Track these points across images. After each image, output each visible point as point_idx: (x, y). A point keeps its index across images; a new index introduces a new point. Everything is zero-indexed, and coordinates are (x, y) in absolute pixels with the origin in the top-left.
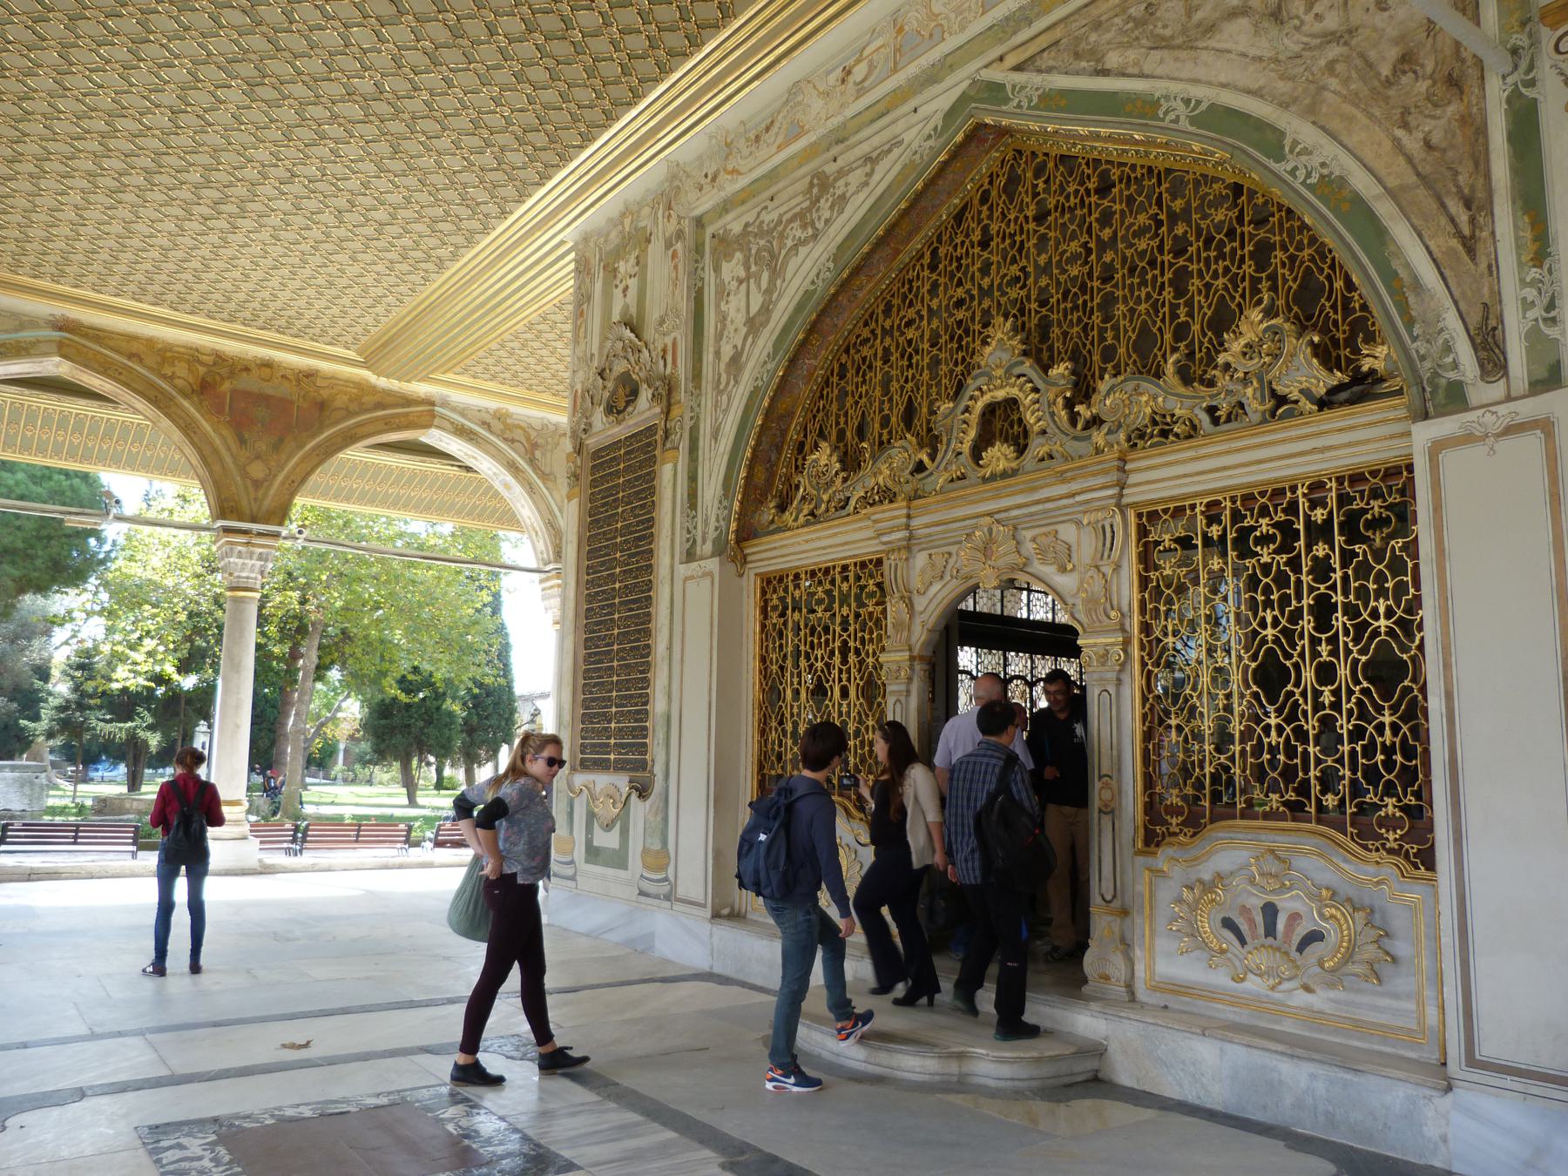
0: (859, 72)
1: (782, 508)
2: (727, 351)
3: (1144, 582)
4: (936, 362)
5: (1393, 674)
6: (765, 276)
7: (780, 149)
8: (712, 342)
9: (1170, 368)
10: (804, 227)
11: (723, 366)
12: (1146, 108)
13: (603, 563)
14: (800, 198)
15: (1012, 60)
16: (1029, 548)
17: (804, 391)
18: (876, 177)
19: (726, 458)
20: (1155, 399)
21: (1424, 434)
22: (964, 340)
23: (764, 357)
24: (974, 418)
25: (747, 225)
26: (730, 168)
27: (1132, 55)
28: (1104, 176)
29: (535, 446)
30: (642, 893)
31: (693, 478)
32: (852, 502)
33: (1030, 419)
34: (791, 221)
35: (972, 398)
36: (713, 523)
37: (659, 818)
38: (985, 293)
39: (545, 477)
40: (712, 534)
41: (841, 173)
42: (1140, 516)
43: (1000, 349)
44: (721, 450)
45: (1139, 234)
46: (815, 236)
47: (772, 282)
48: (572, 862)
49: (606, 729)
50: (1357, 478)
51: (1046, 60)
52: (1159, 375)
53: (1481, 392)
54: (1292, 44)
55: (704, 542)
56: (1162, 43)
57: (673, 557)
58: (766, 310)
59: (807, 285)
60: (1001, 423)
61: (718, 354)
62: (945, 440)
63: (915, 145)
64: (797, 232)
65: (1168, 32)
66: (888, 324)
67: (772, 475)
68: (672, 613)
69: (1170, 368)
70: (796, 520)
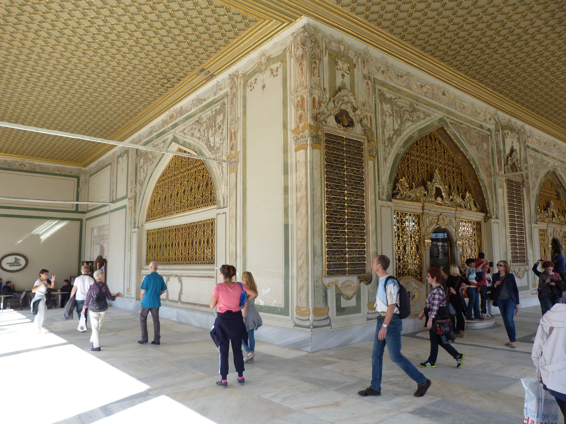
2: (387, 135)
6: (399, 120)
7: (405, 87)
11: (386, 139)
12: (467, 151)
13: (337, 186)
14: (408, 106)
18: (426, 120)
24: (434, 188)
26: (389, 75)
30: (368, 319)
33: (443, 194)
36: (386, 190)
44: (388, 166)
48: (328, 318)
49: (343, 258)
52: (459, 195)
53: (493, 217)
55: (383, 194)
56: (467, 140)
57: (375, 196)
60: (438, 193)
61: (383, 132)
62: (430, 191)
63: (434, 120)
68: (376, 216)
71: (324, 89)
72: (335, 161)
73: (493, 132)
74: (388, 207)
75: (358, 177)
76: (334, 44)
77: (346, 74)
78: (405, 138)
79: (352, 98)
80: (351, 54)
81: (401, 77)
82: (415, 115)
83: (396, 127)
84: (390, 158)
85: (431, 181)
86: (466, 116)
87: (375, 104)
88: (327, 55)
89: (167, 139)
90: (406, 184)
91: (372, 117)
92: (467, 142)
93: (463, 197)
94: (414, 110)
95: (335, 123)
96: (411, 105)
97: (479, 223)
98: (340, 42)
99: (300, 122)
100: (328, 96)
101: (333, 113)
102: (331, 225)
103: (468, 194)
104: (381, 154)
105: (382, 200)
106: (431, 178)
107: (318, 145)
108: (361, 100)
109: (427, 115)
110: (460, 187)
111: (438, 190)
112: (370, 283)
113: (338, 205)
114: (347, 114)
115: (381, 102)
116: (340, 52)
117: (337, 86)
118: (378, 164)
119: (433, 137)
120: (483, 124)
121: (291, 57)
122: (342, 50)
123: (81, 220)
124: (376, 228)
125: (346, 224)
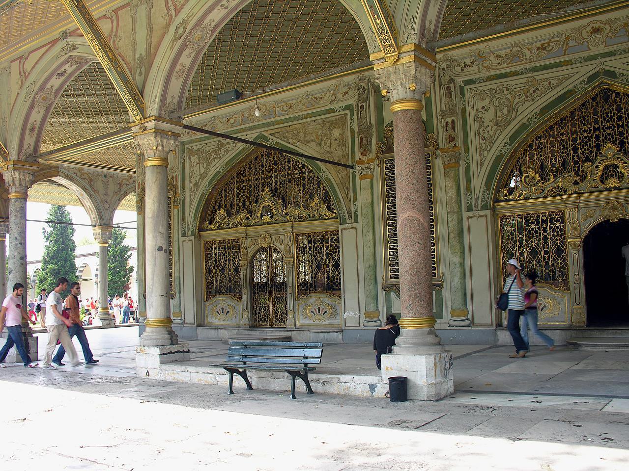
0: (232, 121)
1: (210, 224)
2: (193, 182)
3: (297, 248)
4: (250, 192)
5: (337, 266)
6: (205, 165)
8: (188, 177)
9: (301, 206)
10: (217, 154)
15: (269, 132)
16: (274, 239)
17: (215, 194)
18: (236, 148)
20: (299, 211)
21: (341, 227)
22: (258, 189)
25: (199, 148)
27: (294, 141)
28: (289, 159)
29: (91, 180)
31: (184, 213)
32: (230, 225)
34: (212, 152)
35: (260, 204)
38: (263, 178)
39: (95, 191)
40: (191, 230)
42: (296, 235)
45: (297, 174)
47: (207, 166)
50: (332, 231)
51: (277, 135)
53: (348, 221)
54: (322, 151)
55: (188, 232)
57: (179, 235)
58: (206, 173)
59: (218, 169)
61: (190, 181)
64: (214, 155)
65: (301, 139)
66: (238, 180)
67: (206, 214)
69: (301, 206)
70: (215, 227)
86: (295, 115)
91: (178, 175)
115: (189, 158)
120: (329, 107)
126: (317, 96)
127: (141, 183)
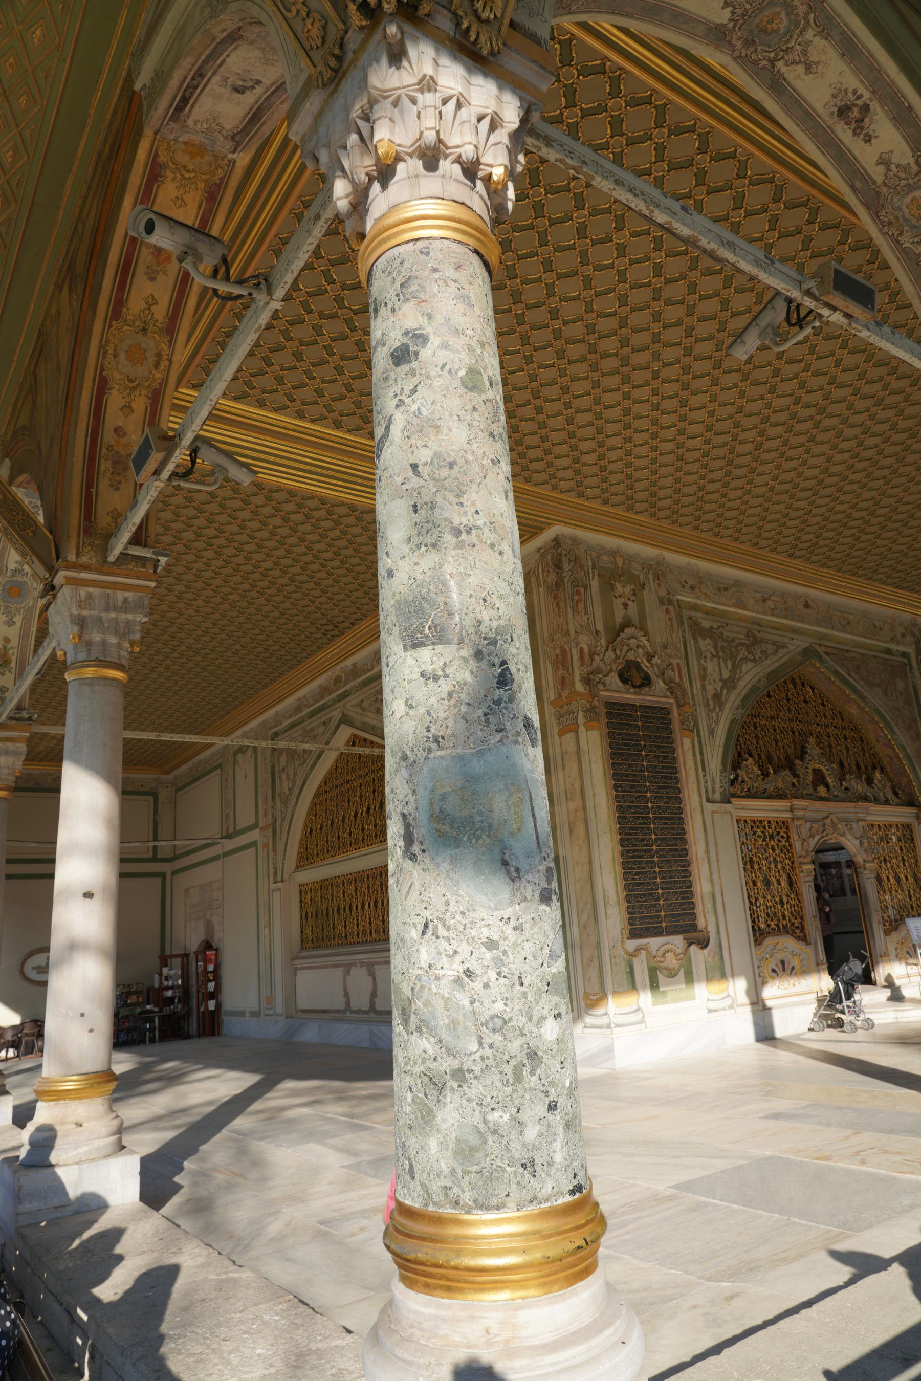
2: (711, 690)
7: (733, 606)
13: (633, 787)
18: (780, 655)
19: (721, 750)
23: (736, 704)
24: (810, 771)
30: (710, 1011)
33: (829, 779)
36: (718, 785)
37: (717, 957)
41: (762, 640)
43: (813, 749)
44: (717, 743)
46: (755, 661)
48: (639, 1009)
49: (655, 905)
55: (714, 792)
57: (700, 796)
60: (819, 779)
61: (703, 687)
68: (705, 831)
71: (597, 632)
72: (626, 745)
73: (913, 656)
74: (725, 812)
75: (668, 768)
76: (605, 558)
77: (630, 603)
78: (744, 692)
79: (643, 639)
80: (636, 569)
81: (726, 589)
82: (758, 650)
83: (726, 675)
84: (720, 728)
85: (802, 759)
87: (685, 643)
88: (596, 577)
89: (330, 719)
90: (756, 769)
92: (862, 683)
93: (870, 781)
94: (756, 641)
95: (620, 684)
96: (749, 633)
97: (908, 827)
98: (615, 553)
99: (563, 689)
100: (603, 642)
101: (614, 667)
102: (628, 851)
103: (878, 775)
104: (703, 725)
105: (714, 802)
106: (802, 754)
107: (595, 724)
108: (658, 639)
109: (779, 646)
110: (862, 764)
111: (817, 772)
112: (706, 946)
113: (638, 818)
114: (637, 665)
116: (617, 568)
117: (618, 624)
118: (700, 742)
119: (797, 680)
121: (539, 585)
122: (620, 565)
123: (163, 875)
124: (707, 852)
125: (655, 848)
126: (877, 623)
127: (586, 650)
